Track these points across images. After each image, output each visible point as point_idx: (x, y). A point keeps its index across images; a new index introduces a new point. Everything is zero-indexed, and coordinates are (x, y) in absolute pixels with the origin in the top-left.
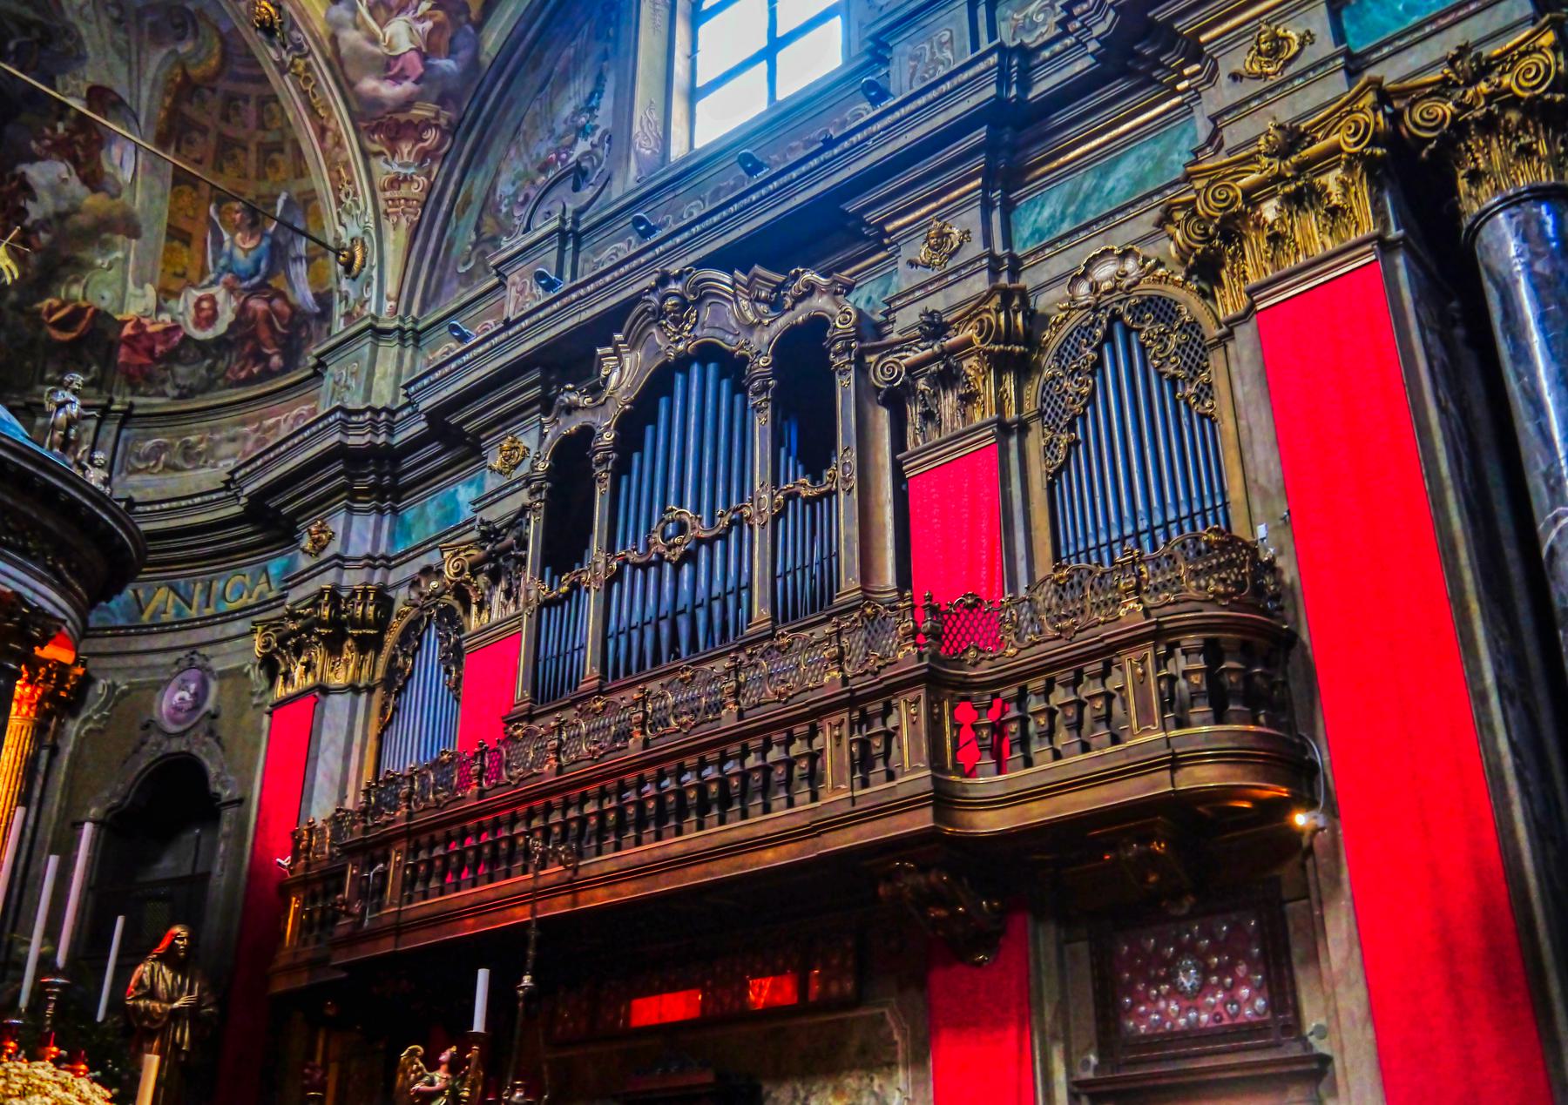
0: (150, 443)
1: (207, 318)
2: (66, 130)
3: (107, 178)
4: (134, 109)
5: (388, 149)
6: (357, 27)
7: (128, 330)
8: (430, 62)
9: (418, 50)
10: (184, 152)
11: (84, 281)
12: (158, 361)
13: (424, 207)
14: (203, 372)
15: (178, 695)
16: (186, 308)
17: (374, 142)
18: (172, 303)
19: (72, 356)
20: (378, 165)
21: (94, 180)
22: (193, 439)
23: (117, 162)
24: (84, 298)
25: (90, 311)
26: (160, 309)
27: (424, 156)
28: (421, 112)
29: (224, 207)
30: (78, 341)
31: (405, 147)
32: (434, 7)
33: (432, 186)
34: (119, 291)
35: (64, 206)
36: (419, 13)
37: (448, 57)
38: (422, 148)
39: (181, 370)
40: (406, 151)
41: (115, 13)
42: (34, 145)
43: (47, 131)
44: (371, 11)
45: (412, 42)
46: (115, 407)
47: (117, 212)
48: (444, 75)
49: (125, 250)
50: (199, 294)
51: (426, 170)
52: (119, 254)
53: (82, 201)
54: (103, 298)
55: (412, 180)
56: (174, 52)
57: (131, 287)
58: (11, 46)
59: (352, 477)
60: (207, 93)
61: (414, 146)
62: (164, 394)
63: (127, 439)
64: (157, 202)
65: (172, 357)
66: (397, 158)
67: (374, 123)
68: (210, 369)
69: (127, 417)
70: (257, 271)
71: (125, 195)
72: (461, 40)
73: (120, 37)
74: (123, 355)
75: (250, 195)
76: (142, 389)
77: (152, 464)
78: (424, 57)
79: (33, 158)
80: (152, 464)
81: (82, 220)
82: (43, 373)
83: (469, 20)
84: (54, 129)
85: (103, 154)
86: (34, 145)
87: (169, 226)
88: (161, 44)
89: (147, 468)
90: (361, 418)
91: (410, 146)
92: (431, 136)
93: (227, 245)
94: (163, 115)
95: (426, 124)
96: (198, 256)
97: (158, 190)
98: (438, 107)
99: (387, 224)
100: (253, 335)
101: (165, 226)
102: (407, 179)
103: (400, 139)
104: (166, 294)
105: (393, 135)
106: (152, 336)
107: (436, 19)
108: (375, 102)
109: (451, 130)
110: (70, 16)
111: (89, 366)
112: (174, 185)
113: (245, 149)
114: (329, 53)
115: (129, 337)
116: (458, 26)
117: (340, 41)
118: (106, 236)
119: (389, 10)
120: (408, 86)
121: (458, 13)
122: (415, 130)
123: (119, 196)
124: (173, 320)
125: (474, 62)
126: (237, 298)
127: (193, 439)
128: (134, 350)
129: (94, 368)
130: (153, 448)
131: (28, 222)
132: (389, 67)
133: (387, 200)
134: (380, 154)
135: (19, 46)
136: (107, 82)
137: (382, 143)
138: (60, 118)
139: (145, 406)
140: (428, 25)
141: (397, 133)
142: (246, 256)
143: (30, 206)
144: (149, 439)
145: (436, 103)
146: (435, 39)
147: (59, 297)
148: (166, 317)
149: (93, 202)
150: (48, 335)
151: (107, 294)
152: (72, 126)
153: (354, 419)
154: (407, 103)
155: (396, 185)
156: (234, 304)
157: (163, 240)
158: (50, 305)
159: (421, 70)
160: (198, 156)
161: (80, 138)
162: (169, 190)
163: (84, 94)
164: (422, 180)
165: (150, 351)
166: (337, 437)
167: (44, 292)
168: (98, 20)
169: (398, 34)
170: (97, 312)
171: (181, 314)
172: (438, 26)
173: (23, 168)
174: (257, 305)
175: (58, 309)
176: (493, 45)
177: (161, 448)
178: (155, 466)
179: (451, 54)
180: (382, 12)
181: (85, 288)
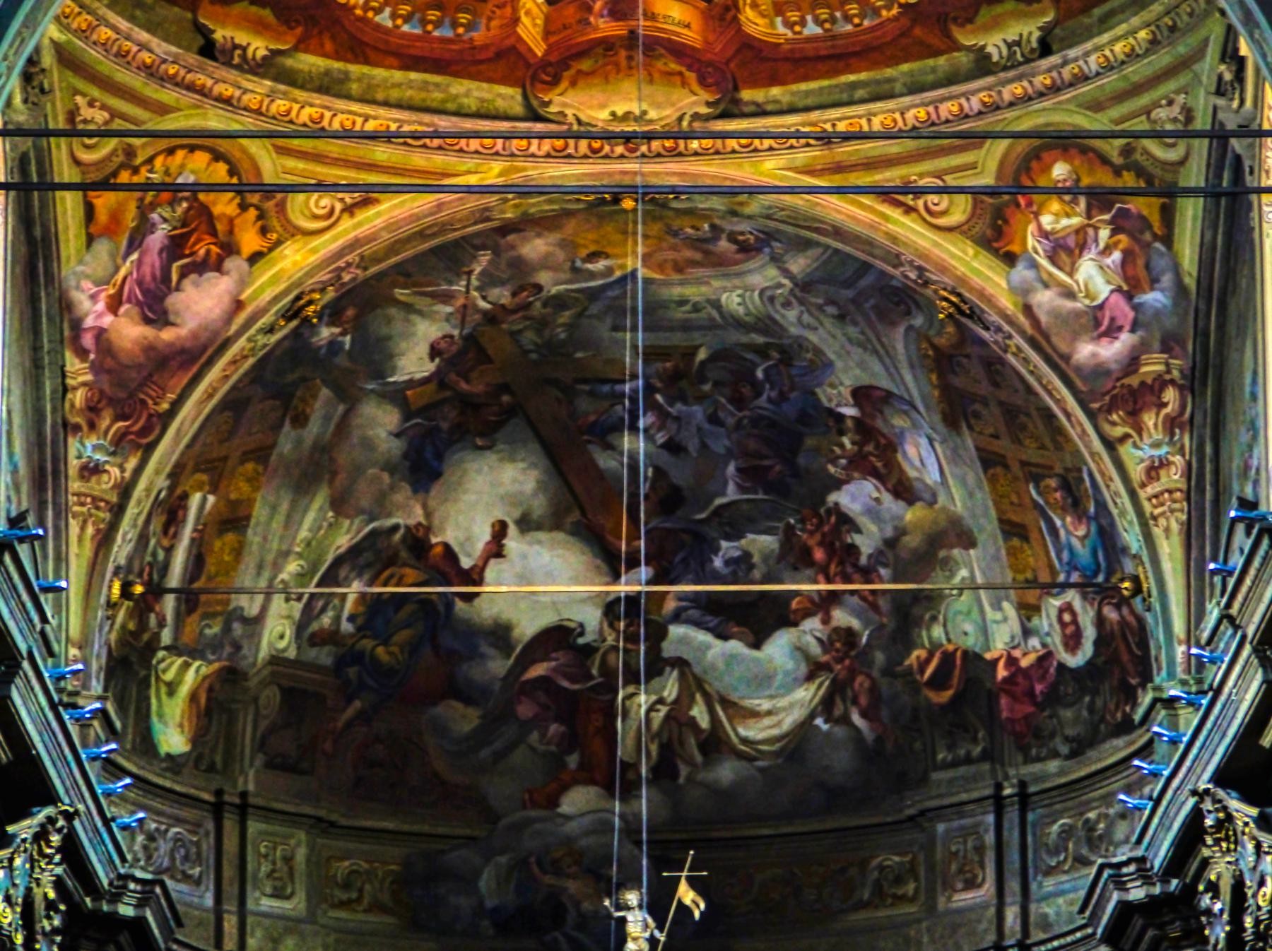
0: (1055, 828)
1: (1073, 641)
2: (853, 443)
3: (917, 485)
4: (907, 397)
5: (1132, 428)
6: (1046, 286)
7: (1002, 673)
8: (1136, 300)
9: (1119, 290)
10: (978, 429)
11: (941, 617)
12: (1041, 707)
13: (1188, 499)
14: (1085, 713)
16: (1051, 625)
17: (1114, 424)
18: (1035, 621)
20: (1126, 451)
21: (905, 491)
22: (1092, 815)
23: (917, 463)
24: (949, 640)
25: (959, 654)
26: (1027, 633)
27: (1171, 424)
28: (1152, 367)
29: (1043, 484)
30: (954, 700)
31: (1149, 419)
32: (1114, 232)
33: (1189, 464)
34: (980, 621)
35: (889, 532)
36: (1102, 245)
37: (1152, 289)
38: (1167, 415)
39: (1067, 714)
40: (1151, 423)
41: (831, 310)
42: (832, 469)
43: (837, 450)
44: (1052, 259)
45: (1109, 282)
46: (1007, 792)
47: (943, 523)
48: (1158, 313)
50: (1056, 603)
51: (1178, 445)
52: (964, 573)
53: (901, 518)
54: (966, 634)
55: (1169, 463)
56: (910, 328)
57: (990, 614)
58: (760, 374)
59: (1161, 927)
60: (965, 361)
61: (1157, 415)
62: (1055, 754)
63: (1034, 825)
64: (979, 495)
65: (1054, 698)
66: (1145, 435)
67: (1107, 398)
68: (1091, 709)
69: (1024, 799)
70: (1098, 565)
71: (942, 500)
72: (1161, 263)
73: (852, 331)
75: (1058, 469)
76: (1034, 752)
77: (1062, 858)
78: (1129, 296)
79: (837, 484)
80: (1062, 858)
81: (912, 541)
82: (934, 754)
83: (1156, 237)
84: (842, 446)
85: (900, 457)
86: (832, 469)
87: (1001, 521)
88: (893, 324)
89: (1059, 863)
90: (1132, 868)
91: (1153, 416)
92: (1170, 395)
93: (1062, 533)
94: (936, 393)
95: (1161, 383)
96: (1042, 554)
97: (971, 479)
98: (1165, 356)
99: (1158, 532)
100: (1114, 659)
101: (996, 523)
102: (1164, 463)
103: (1141, 410)
105: (1130, 409)
106: (1025, 672)
107: (1121, 246)
108: (1099, 371)
109: (1192, 384)
110: (794, 330)
111: (976, 732)
112: (985, 472)
113: (1028, 415)
114: (1029, 330)
115: (1005, 680)
116: (1147, 246)
117: (1036, 310)
118: (942, 553)
119: (1070, 252)
120: (1125, 340)
121: (1142, 232)
122: (1149, 394)
123: (935, 502)
124: (1044, 645)
125: (1180, 289)
126: (1092, 605)
127: (1092, 815)
128: (1014, 697)
129: (980, 735)
130: (1059, 834)
131: (863, 560)
133: (1149, 499)
134: (1126, 437)
135: (766, 371)
136: (866, 380)
137: (1125, 423)
138: (841, 433)
139: (1039, 779)
140: (1117, 255)
141: (1135, 403)
142: (1084, 546)
143: (857, 539)
144: (1054, 822)
145: (1162, 352)
146: (1130, 272)
147: (923, 647)
148: (1034, 642)
149: (911, 515)
150: (927, 699)
151: (968, 627)
152: (857, 438)
153: (1125, 870)
154: (1133, 362)
155: (1153, 474)
156: (1092, 613)
157: (1001, 541)
158: (918, 657)
159: (1131, 314)
160: (991, 430)
161: (870, 448)
162: (982, 476)
163: (851, 401)
164: (1178, 459)
165: (1031, 693)
166: (1115, 896)
167: (910, 645)
168: (821, 324)
169: (1090, 277)
170: (966, 653)
171: (1048, 634)
172: (1127, 254)
173: (833, 498)
174: (1111, 614)
175: (928, 661)
176: (1191, 260)
177: (1067, 833)
178: (1066, 859)
179: (1154, 282)
180: (1064, 257)
181: (945, 626)
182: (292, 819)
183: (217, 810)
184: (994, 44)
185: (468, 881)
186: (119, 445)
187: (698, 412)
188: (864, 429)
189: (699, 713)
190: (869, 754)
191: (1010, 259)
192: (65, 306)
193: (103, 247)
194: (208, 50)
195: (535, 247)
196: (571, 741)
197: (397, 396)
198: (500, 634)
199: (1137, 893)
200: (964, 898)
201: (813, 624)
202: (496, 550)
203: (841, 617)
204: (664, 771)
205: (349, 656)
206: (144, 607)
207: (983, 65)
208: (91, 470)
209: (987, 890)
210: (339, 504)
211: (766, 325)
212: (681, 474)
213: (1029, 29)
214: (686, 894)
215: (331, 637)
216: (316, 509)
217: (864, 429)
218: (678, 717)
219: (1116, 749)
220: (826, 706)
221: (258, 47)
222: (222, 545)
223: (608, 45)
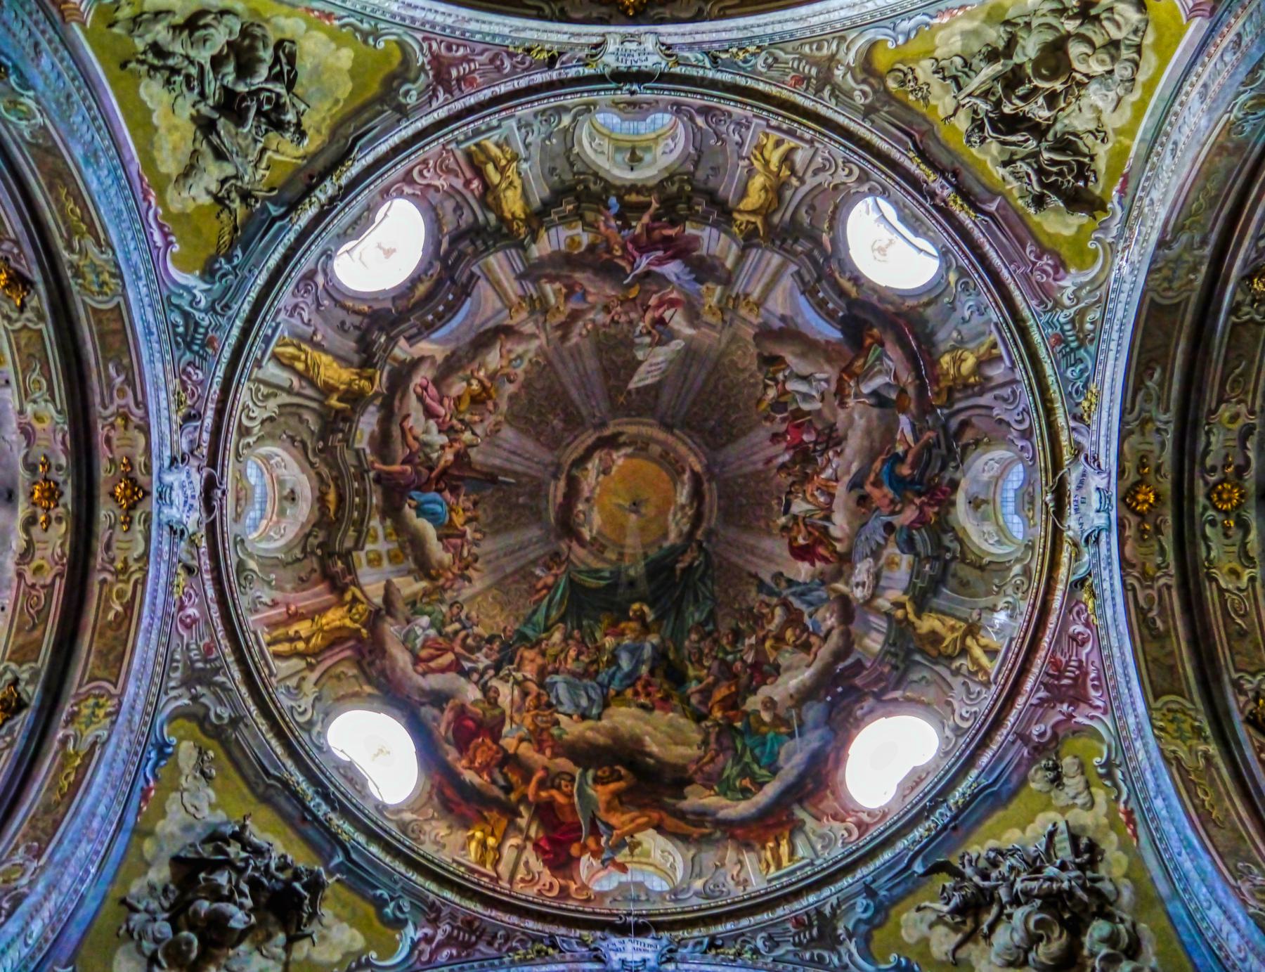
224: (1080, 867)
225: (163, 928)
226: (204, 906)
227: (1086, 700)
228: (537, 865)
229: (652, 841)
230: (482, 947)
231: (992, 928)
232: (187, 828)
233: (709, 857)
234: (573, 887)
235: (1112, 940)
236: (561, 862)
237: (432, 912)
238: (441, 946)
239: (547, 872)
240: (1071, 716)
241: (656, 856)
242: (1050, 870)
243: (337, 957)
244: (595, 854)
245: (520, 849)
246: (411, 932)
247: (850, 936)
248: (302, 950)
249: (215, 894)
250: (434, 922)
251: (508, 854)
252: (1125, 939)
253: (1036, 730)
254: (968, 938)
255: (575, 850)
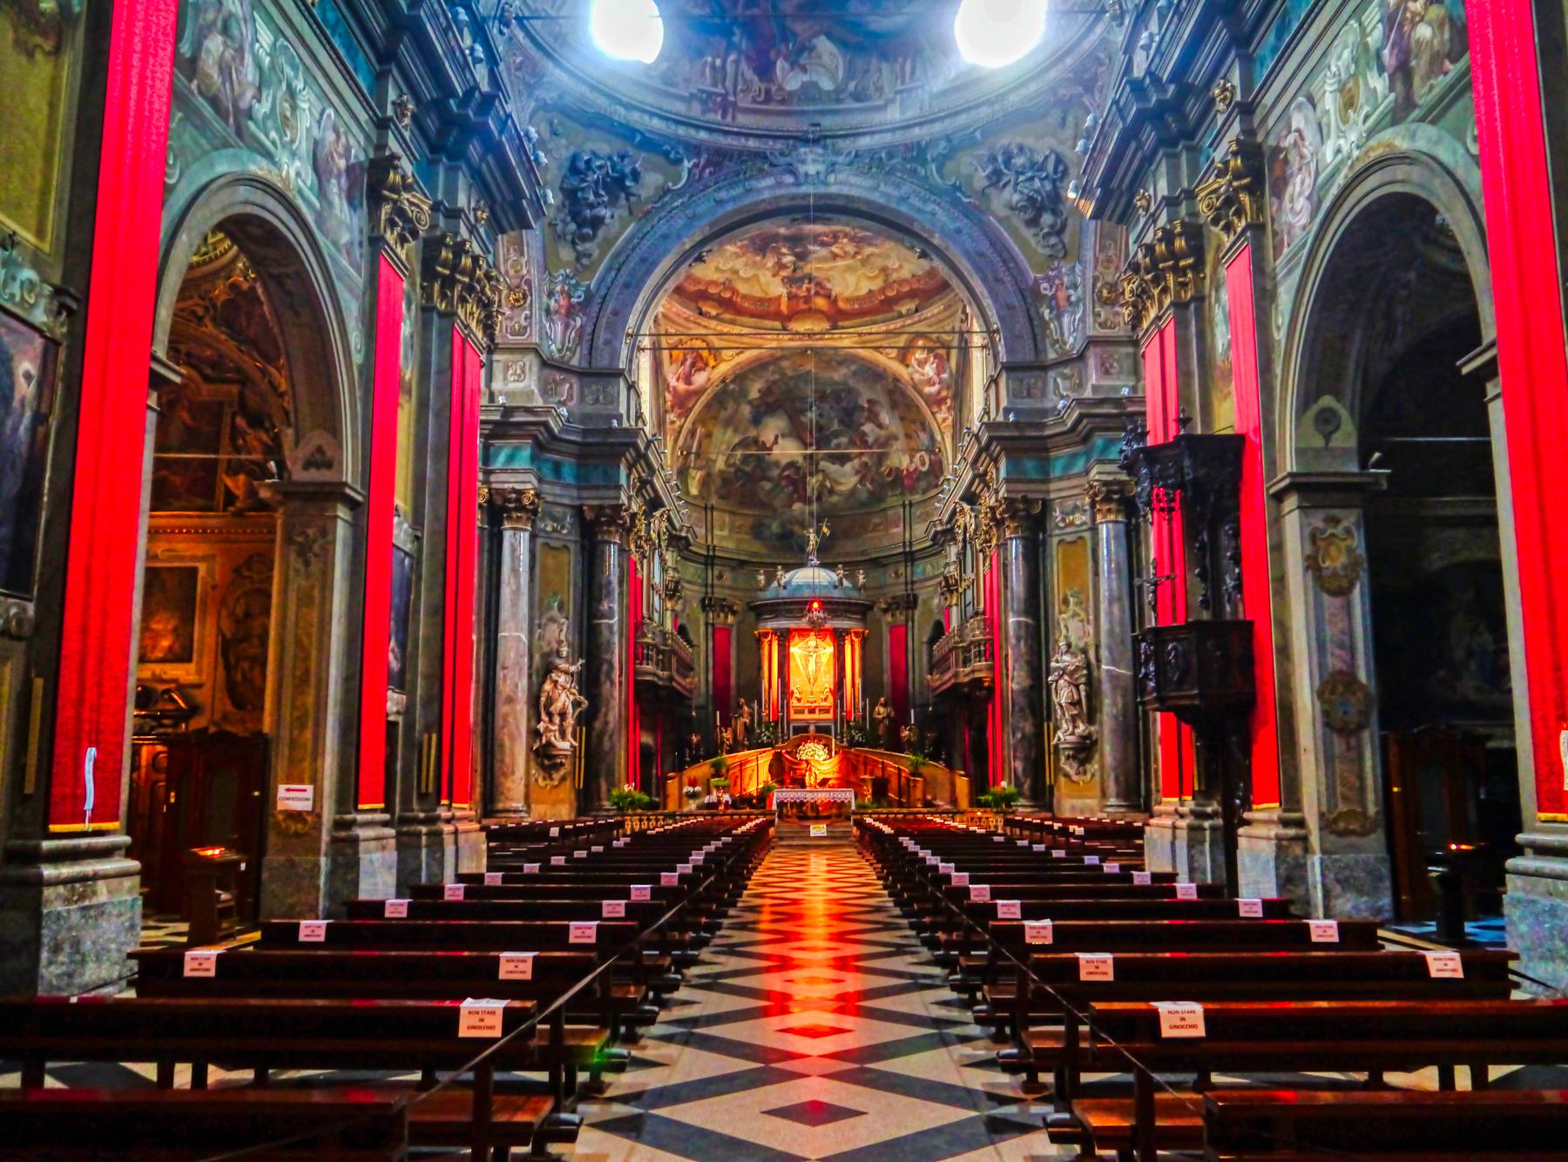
1: (923, 464)
15: (936, 601)
19: (893, 484)
21: (880, 426)
28: (944, 394)
31: (944, 408)
49: (897, 445)
65: (918, 479)
74: (906, 482)
104: (912, 457)
108: (930, 395)
120: (937, 387)
122: (943, 400)
132: (930, 382)
149: (883, 433)
154: (939, 392)
182: (724, 511)
183: (706, 508)
184: (904, 310)
185: (769, 527)
186: (679, 416)
187: (826, 407)
188: (870, 410)
189: (828, 484)
190: (871, 494)
191: (907, 366)
192: (665, 380)
193: (674, 366)
194: (701, 313)
195: (785, 364)
196: (795, 491)
197: (750, 402)
198: (777, 464)
199: (939, 528)
200: (895, 530)
201: (856, 462)
202: (776, 442)
203: (865, 459)
204: (819, 498)
205: (738, 470)
206: (686, 457)
207: (901, 316)
208: (673, 422)
209: (900, 529)
210: (736, 431)
211: (845, 383)
212: (823, 422)
213: (912, 306)
214: (825, 529)
215: (734, 465)
216: (729, 432)
217: (870, 410)
218: (822, 485)
219: (933, 493)
220: (861, 481)
221: (714, 312)
222: (705, 442)
223: (803, 311)
224: (1054, 182)
225: (573, 227)
226: (588, 212)
227: (1092, 94)
228: (749, 74)
229: (824, 45)
230: (727, 163)
231: (1005, 186)
232: (560, 168)
233: (860, 63)
234: (774, 88)
235: (1052, 226)
236: (765, 70)
237: (695, 149)
238: (704, 168)
239: (756, 78)
240: (1081, 96)
241: (826, 59)
242: (1037, 183)
243: (651, 192)
244: (786, 59)
245: (737, 63)
246: (687, 164)
247: (933, 160)
248: (633, 199)
249: (592, 207)
250: (698, 155)
251: (730, 69)
252: (1058, 227)
253: (1062, 91)
254: (994, 185)
255: (772, 54)
